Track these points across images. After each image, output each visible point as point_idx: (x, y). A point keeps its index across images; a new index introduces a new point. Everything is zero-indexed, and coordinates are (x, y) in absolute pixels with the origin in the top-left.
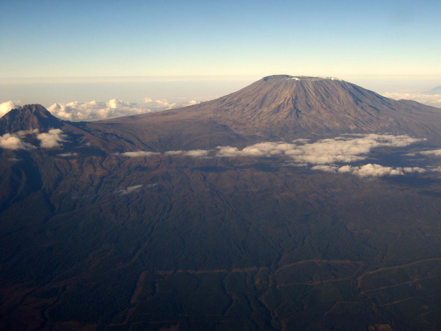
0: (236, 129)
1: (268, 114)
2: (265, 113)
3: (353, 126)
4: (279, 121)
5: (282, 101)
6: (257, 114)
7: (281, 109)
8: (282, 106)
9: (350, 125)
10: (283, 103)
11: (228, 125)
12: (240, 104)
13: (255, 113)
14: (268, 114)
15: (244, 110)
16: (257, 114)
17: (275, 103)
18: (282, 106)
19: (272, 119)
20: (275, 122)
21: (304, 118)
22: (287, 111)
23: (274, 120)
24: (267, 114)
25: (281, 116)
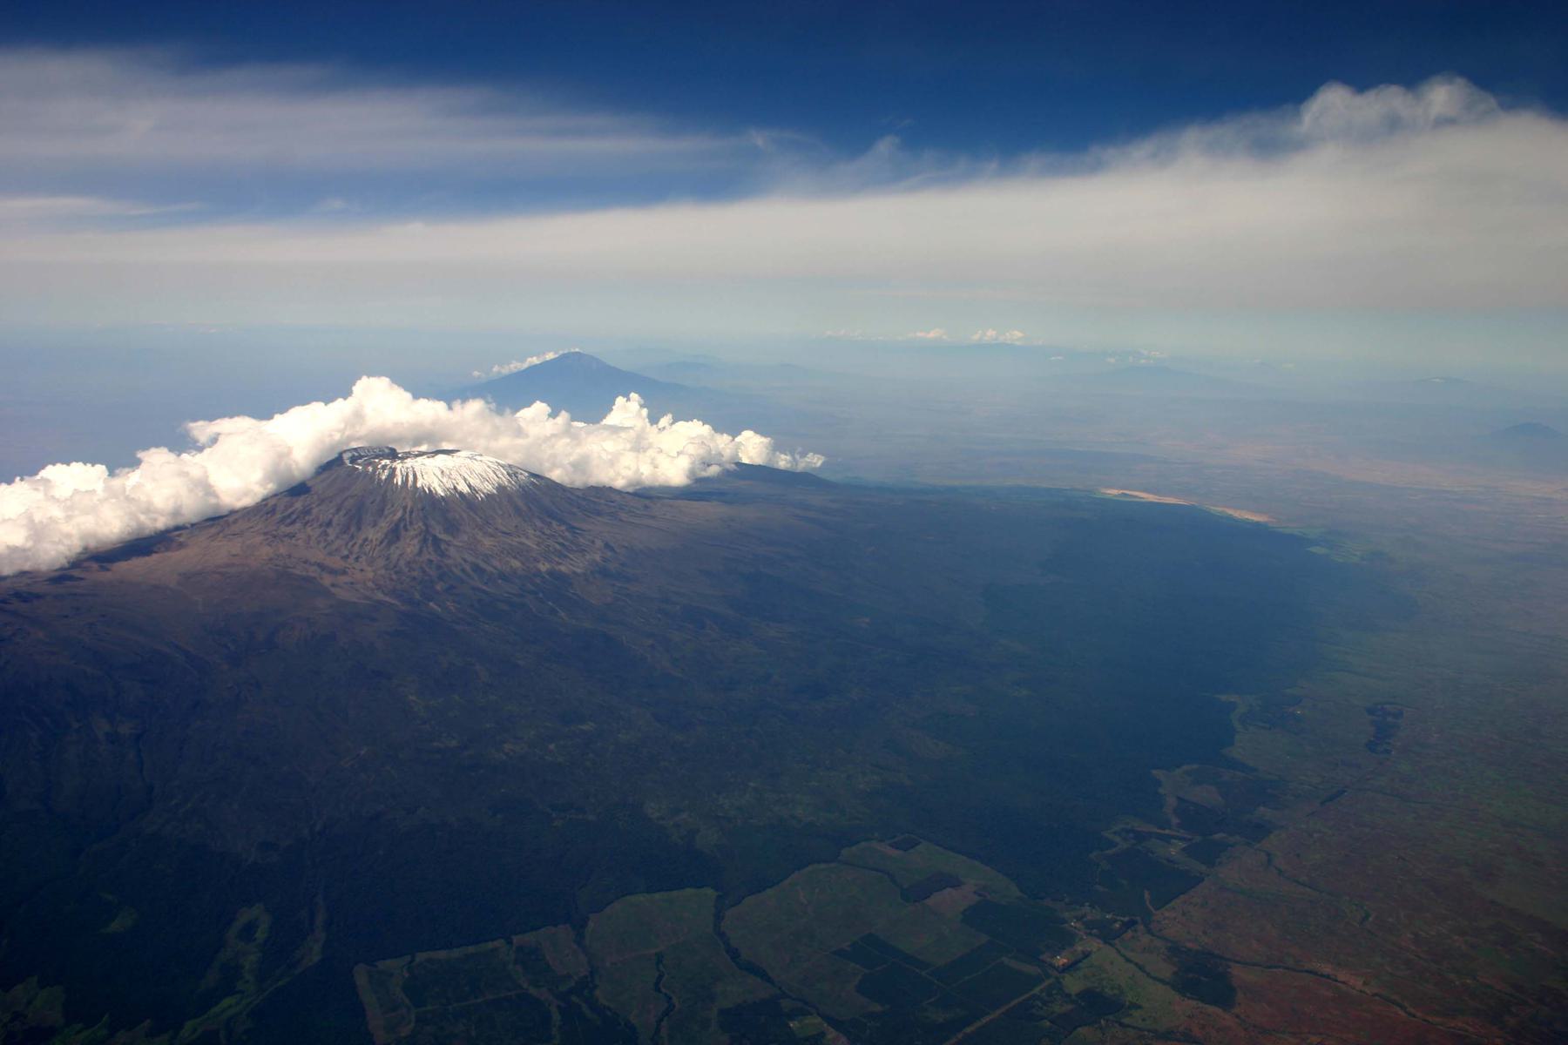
0: (333, 585)
1: (381, 543)
2: (374, 543)
3: (544, 564)
4: (409, 563)
5: (399, 514)
6: (358, 545)
7: (403, 533)
8: (402, 525)
9: (538, 562)
10: (401, 520)
11: (313, 575)
12: (313, 520)
13: (354, 542)
14: (381, 543)
15: (326, 534)
16: (358, 545)
17: (386, 517)
18: (402, 525)
19: (394, 557)
20: (402, 563)
21: (452, 551)
22: (416, 536)
23: (398, 560)
24: (379, 545)
25: (409, 550)
